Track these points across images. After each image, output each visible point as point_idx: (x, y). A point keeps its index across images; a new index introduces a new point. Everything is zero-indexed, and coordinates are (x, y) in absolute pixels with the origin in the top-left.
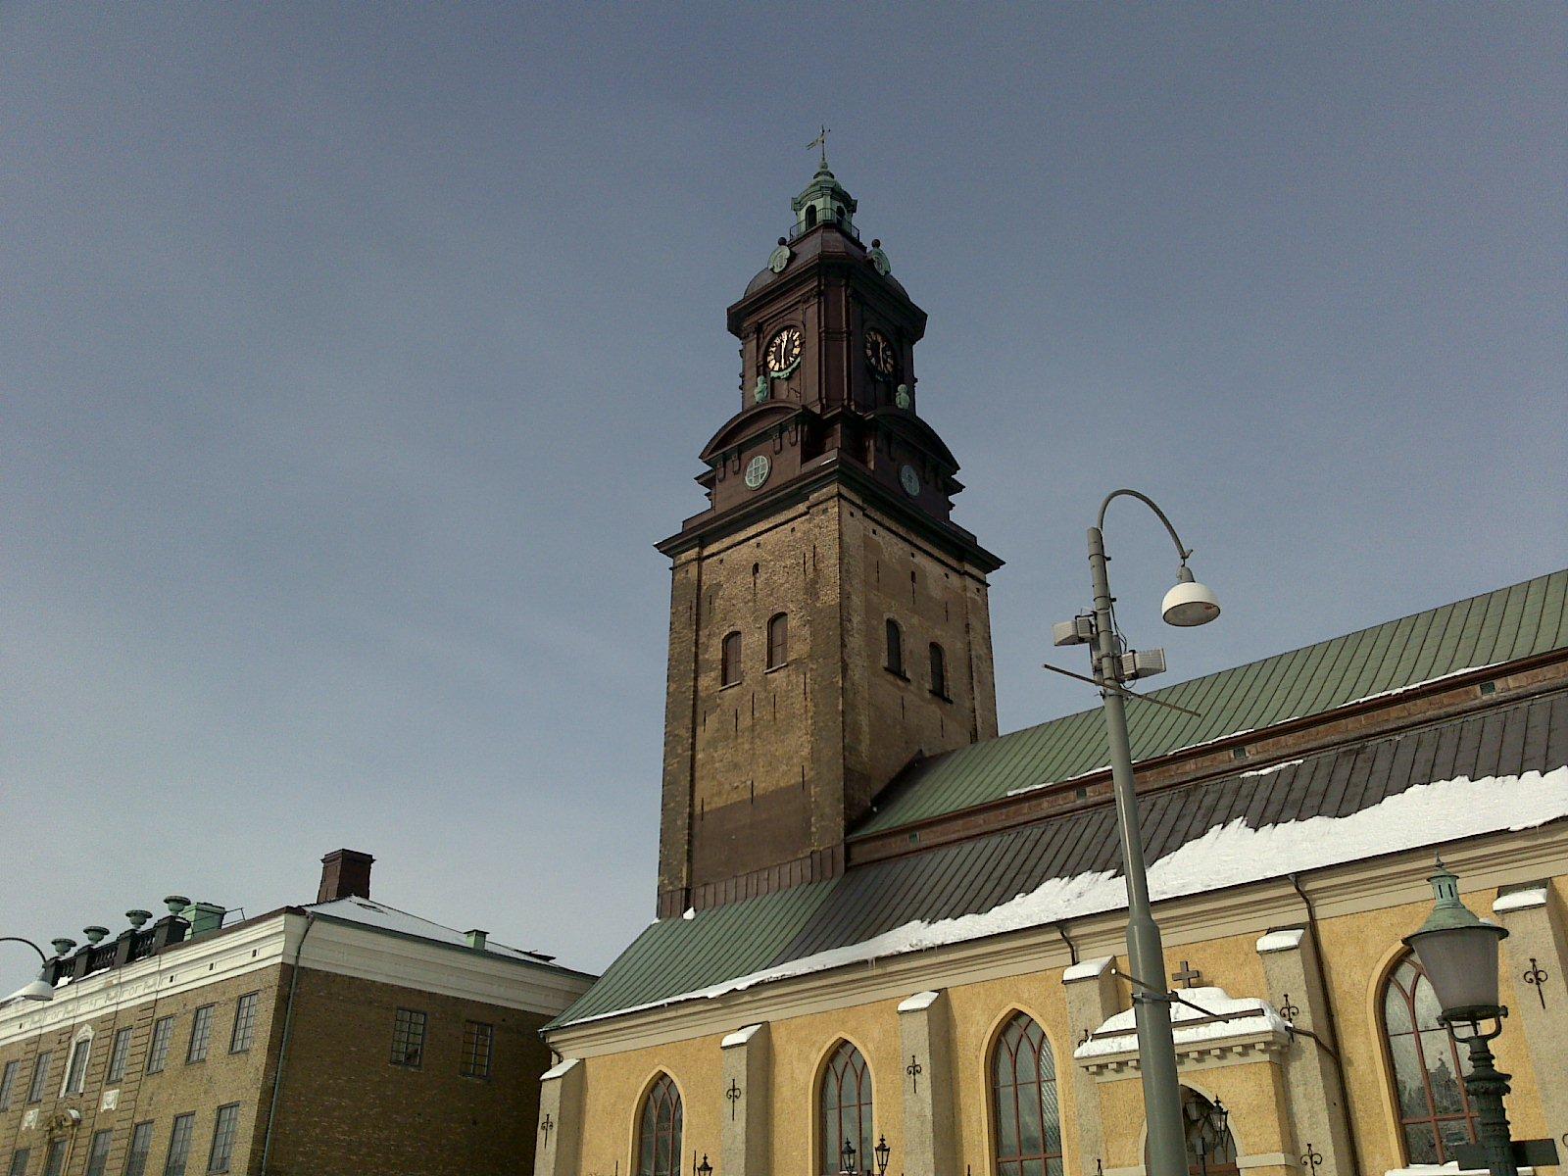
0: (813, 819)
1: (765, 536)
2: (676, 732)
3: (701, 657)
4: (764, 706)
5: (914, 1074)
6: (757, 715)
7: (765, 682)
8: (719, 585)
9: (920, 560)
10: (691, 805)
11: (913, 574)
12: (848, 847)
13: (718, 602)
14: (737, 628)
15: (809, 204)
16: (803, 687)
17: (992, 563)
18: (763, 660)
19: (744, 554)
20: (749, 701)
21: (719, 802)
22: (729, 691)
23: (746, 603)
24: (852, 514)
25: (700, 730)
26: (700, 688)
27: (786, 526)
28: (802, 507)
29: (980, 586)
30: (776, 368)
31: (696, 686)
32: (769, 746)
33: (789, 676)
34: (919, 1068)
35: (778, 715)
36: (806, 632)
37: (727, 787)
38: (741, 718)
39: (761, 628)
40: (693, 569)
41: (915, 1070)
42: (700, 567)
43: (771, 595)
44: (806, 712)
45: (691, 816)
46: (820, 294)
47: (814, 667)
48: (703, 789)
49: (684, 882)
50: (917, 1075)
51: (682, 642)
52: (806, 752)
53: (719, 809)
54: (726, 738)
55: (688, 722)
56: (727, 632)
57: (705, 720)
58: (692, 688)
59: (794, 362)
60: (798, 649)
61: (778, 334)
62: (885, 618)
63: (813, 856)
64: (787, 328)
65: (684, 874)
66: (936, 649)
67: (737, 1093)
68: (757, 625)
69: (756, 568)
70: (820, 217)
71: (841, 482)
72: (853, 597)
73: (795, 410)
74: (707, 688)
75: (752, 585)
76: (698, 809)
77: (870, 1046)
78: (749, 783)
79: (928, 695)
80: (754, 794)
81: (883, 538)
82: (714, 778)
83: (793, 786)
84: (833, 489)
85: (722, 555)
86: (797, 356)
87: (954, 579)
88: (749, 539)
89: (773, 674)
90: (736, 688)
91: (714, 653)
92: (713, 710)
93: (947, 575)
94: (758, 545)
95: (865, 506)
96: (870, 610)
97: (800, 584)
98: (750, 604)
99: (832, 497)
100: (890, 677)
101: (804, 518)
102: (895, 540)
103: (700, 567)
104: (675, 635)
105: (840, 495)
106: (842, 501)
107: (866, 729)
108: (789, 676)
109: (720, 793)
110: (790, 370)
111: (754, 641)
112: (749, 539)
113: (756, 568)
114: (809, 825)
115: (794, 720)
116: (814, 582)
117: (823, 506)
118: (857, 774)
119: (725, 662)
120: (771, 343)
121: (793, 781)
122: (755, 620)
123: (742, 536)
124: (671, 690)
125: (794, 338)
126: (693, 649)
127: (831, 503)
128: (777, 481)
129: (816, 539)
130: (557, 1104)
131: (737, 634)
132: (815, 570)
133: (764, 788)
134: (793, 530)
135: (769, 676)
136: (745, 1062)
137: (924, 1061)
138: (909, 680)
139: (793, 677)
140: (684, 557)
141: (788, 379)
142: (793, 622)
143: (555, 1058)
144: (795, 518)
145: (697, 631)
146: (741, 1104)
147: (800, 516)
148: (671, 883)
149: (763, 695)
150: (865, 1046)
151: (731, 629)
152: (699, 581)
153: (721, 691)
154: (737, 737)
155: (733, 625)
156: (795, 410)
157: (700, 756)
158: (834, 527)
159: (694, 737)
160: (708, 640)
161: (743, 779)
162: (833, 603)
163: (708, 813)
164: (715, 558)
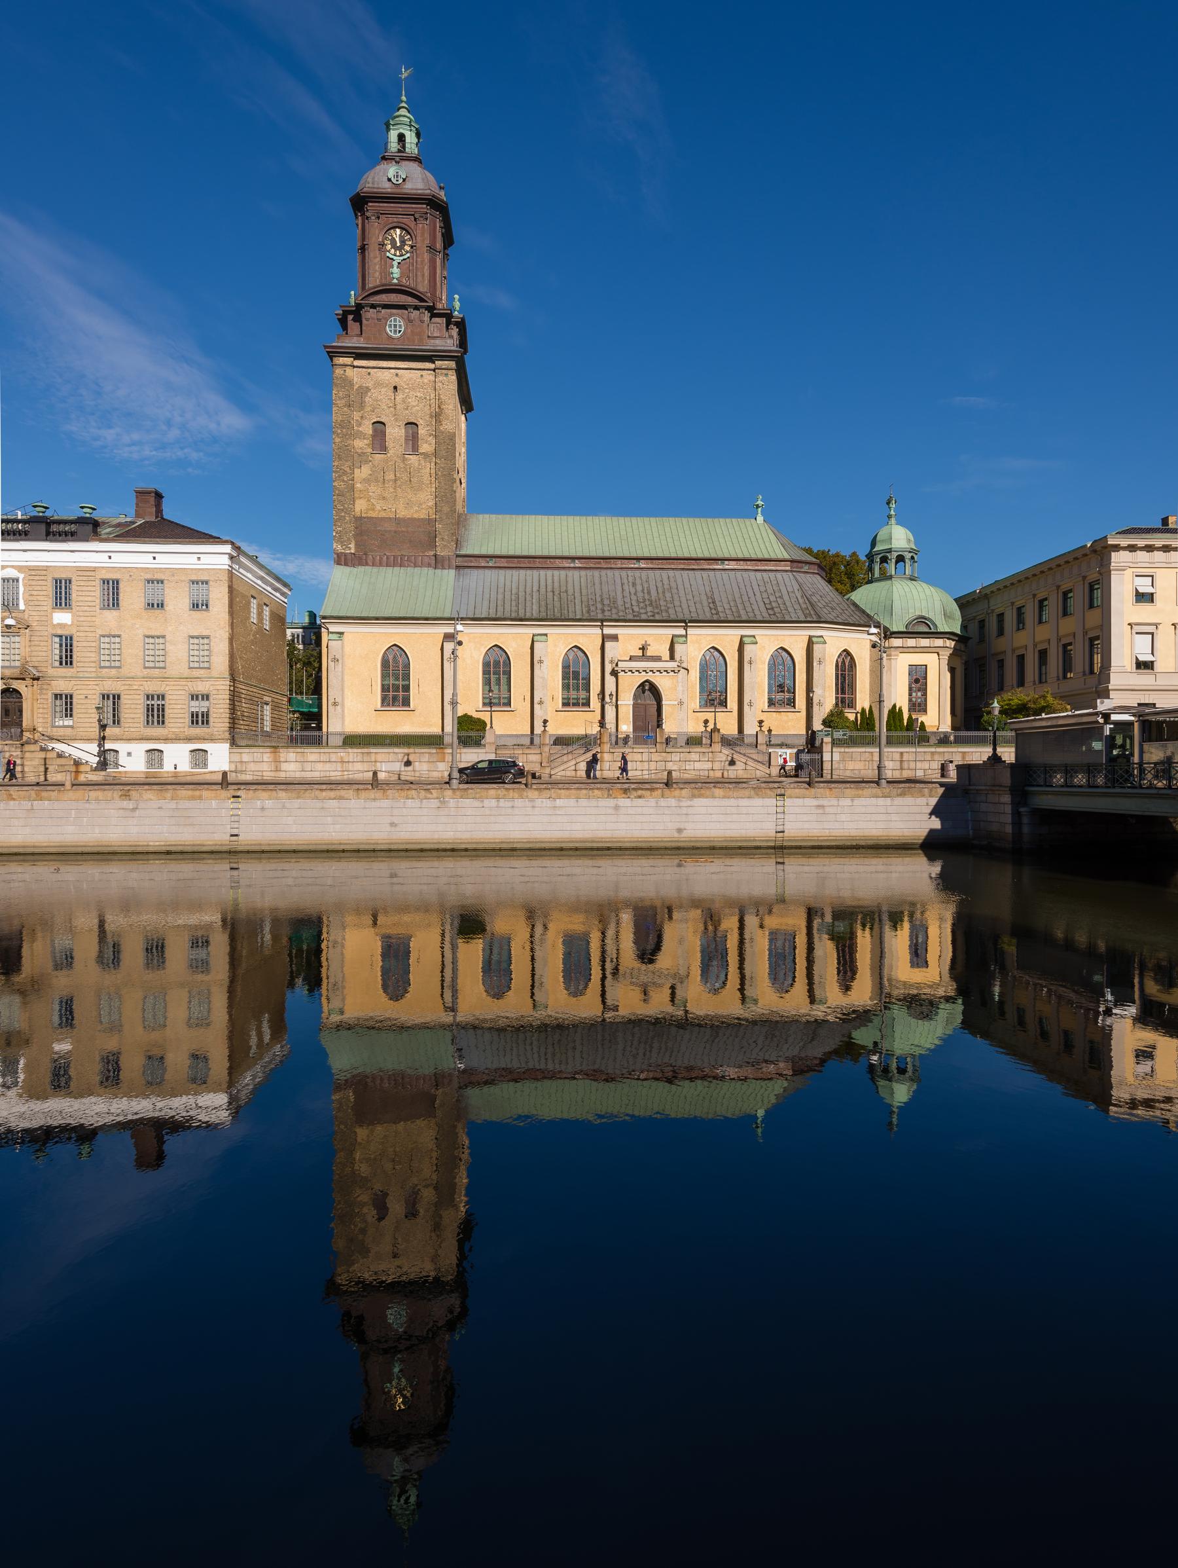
54: (377, 481)
65: (352, 546)
69: (395, 388)
73: (427, 302)
75: (393, 398)
82: (369, 500)
92: (367, 462)
111: (395, 433)
113: (395, 388)
122: (396, 420)
134: (422, 376)
144: (424, 370)
147: (427, 370)
163: (365, 518)
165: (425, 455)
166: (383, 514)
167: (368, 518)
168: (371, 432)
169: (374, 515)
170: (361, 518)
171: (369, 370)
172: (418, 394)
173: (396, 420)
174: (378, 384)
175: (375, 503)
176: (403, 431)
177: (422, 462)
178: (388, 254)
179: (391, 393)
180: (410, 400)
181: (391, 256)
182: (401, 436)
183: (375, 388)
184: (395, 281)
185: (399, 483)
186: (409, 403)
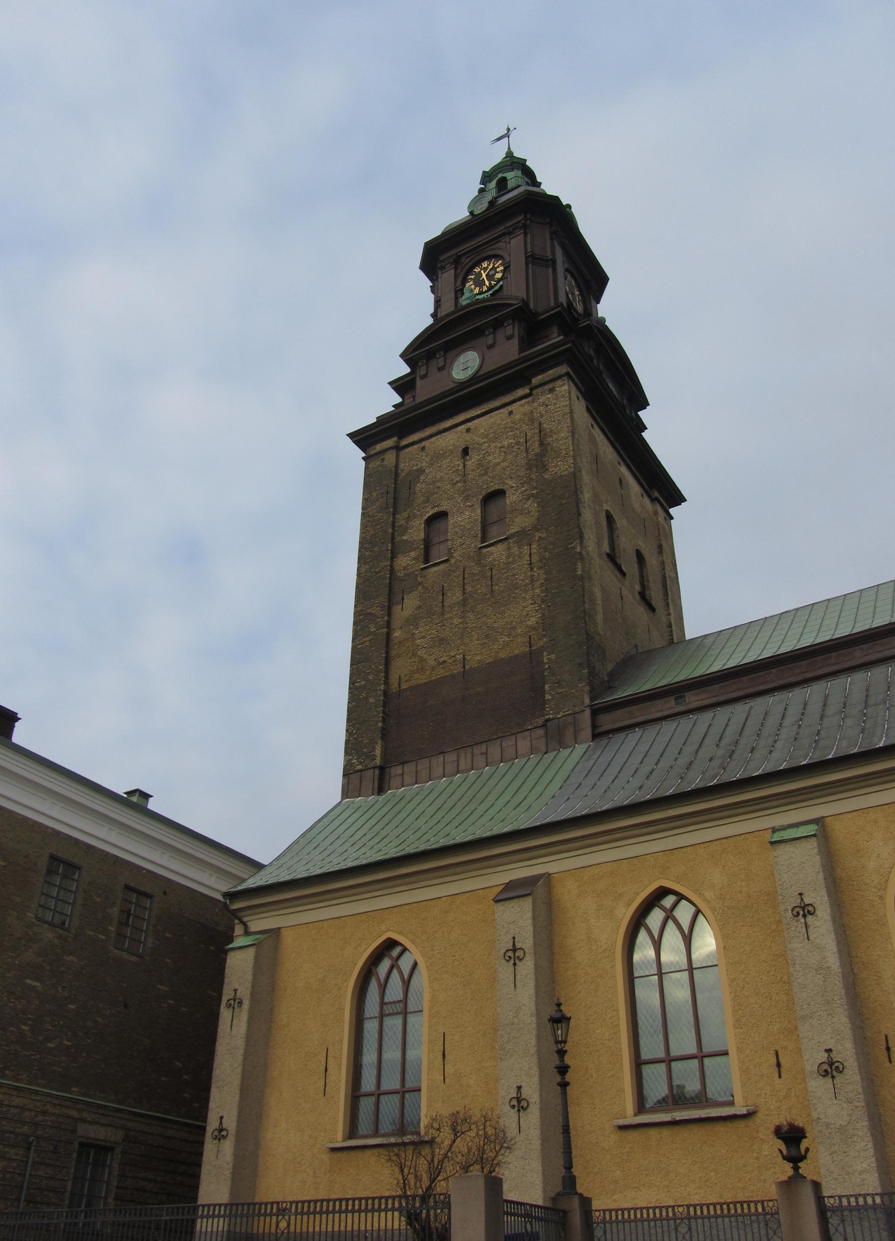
0: (546, 687)
2: (369, 611)
3: (398, 539)
4: (478, 580)
5: (804, 916)
6: (469, 589)
8: (421, 471)
9: (623, 470)
10: (386, 683)
11: (620, 479)
14: (442, 509)
15: (500, 175)
16: (527, 557)
17: (676, 498)
18: (475, 537)
19: (452, 440)
21: (421, 679)
23: (454, 484)
24: (578, 398)
25: (397, 609)
26: (397, 568)
27: (502, 410)
29: (667, 517)
31: (392, 566)
32: (484, 619)
33: (509, 549)
34: (810, 909)
36: (532, 506)
39: (472, 506)
40: (390, 458)
41: (805, 910)
42: (398, 456)
43: (486, 473)
44: (532, 581)
45: (385, 693)
46: (525, 227)
48: (401, 668)
49: (378, 761)
50: (809, 918)
52: (532, 621)
55: (383, 599)
56: (431, 513)
57: (403, 599)
58: (389, 568)
59: (495, 285)
61: (478, 263)
63: (548, 724)
64: (488, 258)
65: (378, 751)
66: (640, 557)
67: (519, 953)
69: (466, 451)
70: (510, 185)
71: (571, 365)
72: (584, 473)
74: (405, 568)
76: (394, 687)
77: (709, 894)
79: (638, 597)
80: (467, 667)
83: (517, 656)
84: (563, 369)
85: (424, 443)
87: (646, 501)
90: (442, 567)
91: (416, 532)
93: (642, 495)
94: (468, 430)
97: (521, 459)
98: (459, 485)
99: (560, 377)
101: (523, 401)
102: (606, 443)
103: (398, 456)
104: (368, 519)
105: (568, 374)
108: (509, 549)
110: (491, 292)
113: (466, 451)
114: (543, 693)
115: (517, 591)
116: (541, 456)
118: (595, 643)
120: (470, 271)
122: (466, 498)
124: (363, 570)
126: (390, 531)
127: (559, 383)
128: (489, 367)
129: (542, 416)
130: (249, 977)
131: (442, 515)
132: (542, 444)
133: (479, 661)
134: (511, 413)
135: (485, 551)
136: (530, 915)
137: (819, 898)
138: (624, 574)
139: (515, 550)
140: (379, 447)
142: (511, 498)
143: (239, 930)
144: (514, 401)
145: (394, 514)
146: (527, 967)
148: (361, 763)
149: (476, 569)
150: (701, 895)
151: (436, 510)
152: (397, 467)
153: (422, 569)
154: (443, 613)
156: (512, 305)
157: (397, 634)
159: (389, 614)
160: (407, 523)
162: (566, 473)
164: (416, 447)
167: (411, 689)
172: (505, 443)
173: (466, 498)
175: (426, 656)
176: (479, 511)
180: (490, 458)
182: (477, 520)
186: (490, 462)
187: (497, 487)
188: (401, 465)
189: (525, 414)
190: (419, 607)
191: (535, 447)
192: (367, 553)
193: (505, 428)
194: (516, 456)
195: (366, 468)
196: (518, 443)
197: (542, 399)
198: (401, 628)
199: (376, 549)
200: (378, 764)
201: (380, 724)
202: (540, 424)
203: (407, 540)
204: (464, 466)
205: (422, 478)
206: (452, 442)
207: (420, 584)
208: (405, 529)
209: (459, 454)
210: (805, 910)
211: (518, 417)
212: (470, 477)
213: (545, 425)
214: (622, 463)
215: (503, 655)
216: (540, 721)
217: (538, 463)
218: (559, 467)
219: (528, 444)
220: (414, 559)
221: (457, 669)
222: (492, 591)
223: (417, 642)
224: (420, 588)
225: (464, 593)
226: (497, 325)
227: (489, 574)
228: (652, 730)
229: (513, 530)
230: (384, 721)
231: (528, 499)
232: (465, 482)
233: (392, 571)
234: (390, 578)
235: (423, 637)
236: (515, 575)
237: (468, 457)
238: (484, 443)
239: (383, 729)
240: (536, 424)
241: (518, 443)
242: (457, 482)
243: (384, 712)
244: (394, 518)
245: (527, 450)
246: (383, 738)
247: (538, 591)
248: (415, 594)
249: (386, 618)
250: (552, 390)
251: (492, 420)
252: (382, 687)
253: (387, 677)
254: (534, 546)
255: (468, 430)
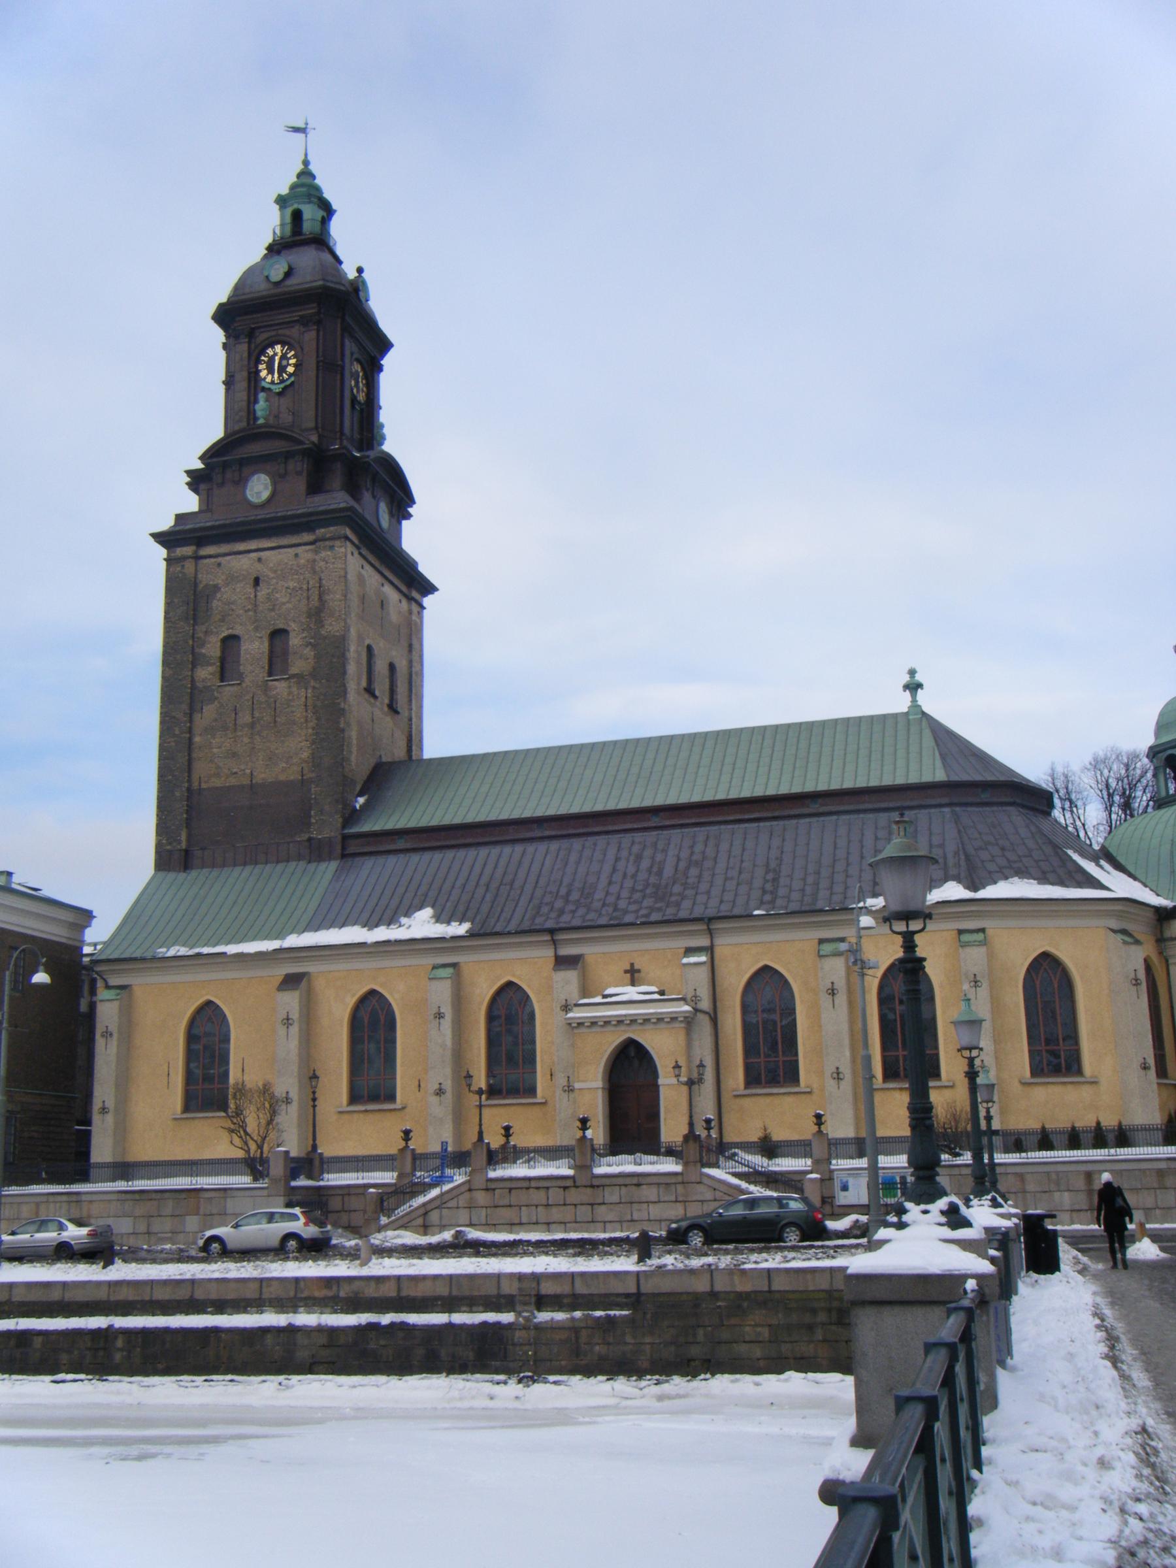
0: (312, 813)
1: (267, 553)
2: (173, 714)
7: (266, 688)
8: (216, 588)
10: (189, 781)
12: (345, 838)
13: (215, 603)
20: (248, 700)
22: (228, 688)
23: (246, 611)
24: (352, 554)
26: (196, 679)
27: (289, 550)
28: (307, 537)
30: (269, 379)
31: (192, 677)
35: (277, 719)
36: (308, 651)
37: (226, 771)
38: (240, 714)
39: (261, 638)
41: (440, 1016)
43: (273, 610)
44: (306, 721)
45: (189, 789)
47: (317, 686)
48: (201, 769)
49: (184, 845)
50: (442, 1020)
51: (178, 633)
52: (305, 755)
53: (217, 788)
60: (298, 666)
62: (367, 642)
65: (184, 837)
68: (258, 635)
69: (257, 581)
74: (203, 681)
76: (195, 785)
78: (248, 771)
80: (254, 782)
81: (368, 572)
86: (290, 375)
88: (249, 551)
89: (276, 683)
90: (235, 688)
91: (212, 649)
92: (213, 699)
94: (260, 560)
95: (361, 546)
96: (360, 638)
98: (251, 613)
100: (366, 696)
106: (348, 543)
107: (355, 742)
109: (217, 775)
111: (254, 648)
112: (249, 551)
113: (257, 581)
114: (310, 817)
117: (328, 543)
119: (223, 660)
121: (292, 778)
122: (256, 629)
123: (241, 546)
125: (289, 356)
126: (191, 642)
127: (337, 543)
129: (322, 572)
131: (233, 638)
133: (263, 779)
134: (296, 555)
135: (270, 683)
137: (447, 1010)
138: (375, 697)
141: (280, 394)
142: (295, 641)
148: (170, 844)
149: (263, 699)
152: (195, 578)
154: (235, 730)
155: (232, 628)
157: (197, 739)
158: (340, 566)
159: (191, 721)
161: (243, 767)
165: (299, 677)
166: (233, 781)
168: (218, 654)
169: (217, 783)
170: (200, 790)
171: (219, 560)
172: (292, 584)
173: (256, 629)
174: (232, 579)
175: (221, 764)
176: (266, 644)
177: (295, 690)
178: (263, 384)
179: (250, 590)
180: (277, 595)
181: (267, 386)
182: (263, 653)
183: (227, 585)
184: (261, 421)
185: (258, 727)
186: (277, 599)
187: (281, 626)
188: (200, 576)
189: (308, 561)
190: (216, 720)
191: (315, 602)
192: (171, 658)
193: (291, 569)
194: (299, 601)
195: (168, 570)
196: (301, 588)
197: (323, 554)
198: (201, 735)
199: (178, 657)
200: (184, 847)
201: (185, 816)
202: (320, 579)
203: (204, 655)
204: (256, 596)
205: (218, 595)
206: (245, 567)
207: (216, 698)
208: (203, 645)
209: (252, 582)
210: (440, 1016)
211: (302, 561)
212: (261, 608)
213: (324, 582)
214: (384, 581)
215: (282, 777)
216: (305, 837)
217: (317, 614)
218: (332, 627)
219: (311, 592)
220: (211, 674)
221: (246, 782)
222: (275, 722)
223: (215, 750)
224: (216, 703)
225: (253, 717)
226: (288, 456)
227: (273, 705)
228: (381, 860)
229: (294, 670)
230: (187, 812)
231: (307, 646)
232: (255, 611)
233: (193, 681)
234: (191, 688)
235: (220, 747)
236: (293, 712)
237: (259, 588)
238: (273, 578)
239: (187, 819)
240: (317, 578)
241: (301, 588)
242: (249, 610)
243: (187, 805)
244: (194, 630)
245: (308, 598)
246: (187, 827)
247: (310, 731)
248: (210, 707)
249: (188, 725)
250: (332, 548)
251: (280, 557)
252: (186, 785)
253: (189, 776)
254: (310, 691)
255: (260, 560)
